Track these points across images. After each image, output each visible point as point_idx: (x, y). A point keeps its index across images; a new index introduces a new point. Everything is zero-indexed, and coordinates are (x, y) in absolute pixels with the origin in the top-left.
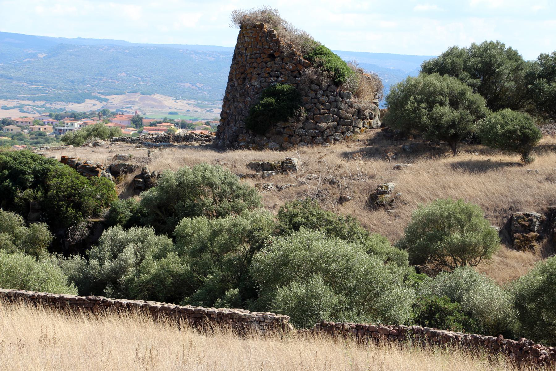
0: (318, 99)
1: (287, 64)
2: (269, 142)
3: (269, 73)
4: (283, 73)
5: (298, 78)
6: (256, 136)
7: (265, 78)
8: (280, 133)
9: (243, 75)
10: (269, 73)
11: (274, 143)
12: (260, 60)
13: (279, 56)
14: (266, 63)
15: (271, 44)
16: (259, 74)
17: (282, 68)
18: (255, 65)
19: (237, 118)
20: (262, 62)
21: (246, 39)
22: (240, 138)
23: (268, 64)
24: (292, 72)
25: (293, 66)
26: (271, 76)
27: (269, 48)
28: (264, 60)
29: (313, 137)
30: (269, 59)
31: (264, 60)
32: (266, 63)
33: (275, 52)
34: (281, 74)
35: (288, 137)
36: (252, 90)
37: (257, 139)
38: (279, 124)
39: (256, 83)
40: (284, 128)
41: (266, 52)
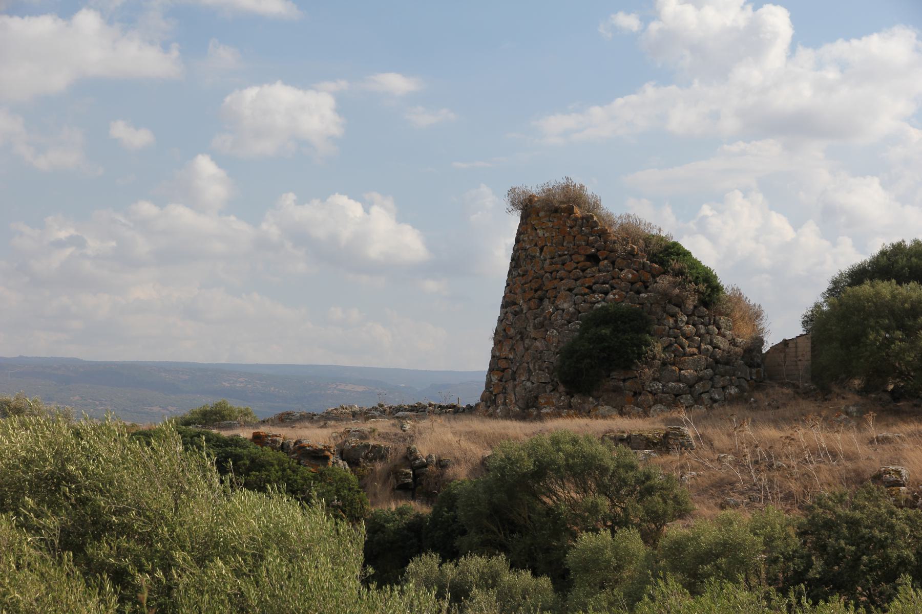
0: (680, 328)
1: (621, 270)
2: (597, 405)
3: (590, 288)
4: (615, 286)
5: (643, 295)
6: (572, 396)
7: (583, 295)
8: (617, 390)
9: (539, 292)
10: (590, 288)
11: (607, 408)
12: (571, 265)
13: (606, 258)
14: (583, 271)
15: (591, 238)
16: (570, 290)
17: (613, 278)
18: (562, 273)
19: (531, 367)
20: (576, 268)
21: (540, 232)
22: (542, 401)
23: (588, 271)
24: (632, 284)
25: (633, 274)
26: (594, 292)
27: (587, 244)
28: (580, 265)
29: (676, 396)
30: (588, 263)
31: (580, 265)
32: (583, 271)
33: (598, 250)
34: (613, 288)
35: (633, 396)
36: (559, 317)
37: (576, 400)
38: (614, 374)
39: (565, 306)
40: (624, 381)
41: (582, 252)
